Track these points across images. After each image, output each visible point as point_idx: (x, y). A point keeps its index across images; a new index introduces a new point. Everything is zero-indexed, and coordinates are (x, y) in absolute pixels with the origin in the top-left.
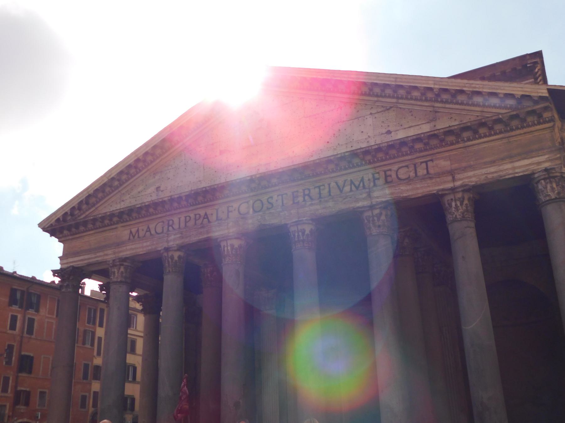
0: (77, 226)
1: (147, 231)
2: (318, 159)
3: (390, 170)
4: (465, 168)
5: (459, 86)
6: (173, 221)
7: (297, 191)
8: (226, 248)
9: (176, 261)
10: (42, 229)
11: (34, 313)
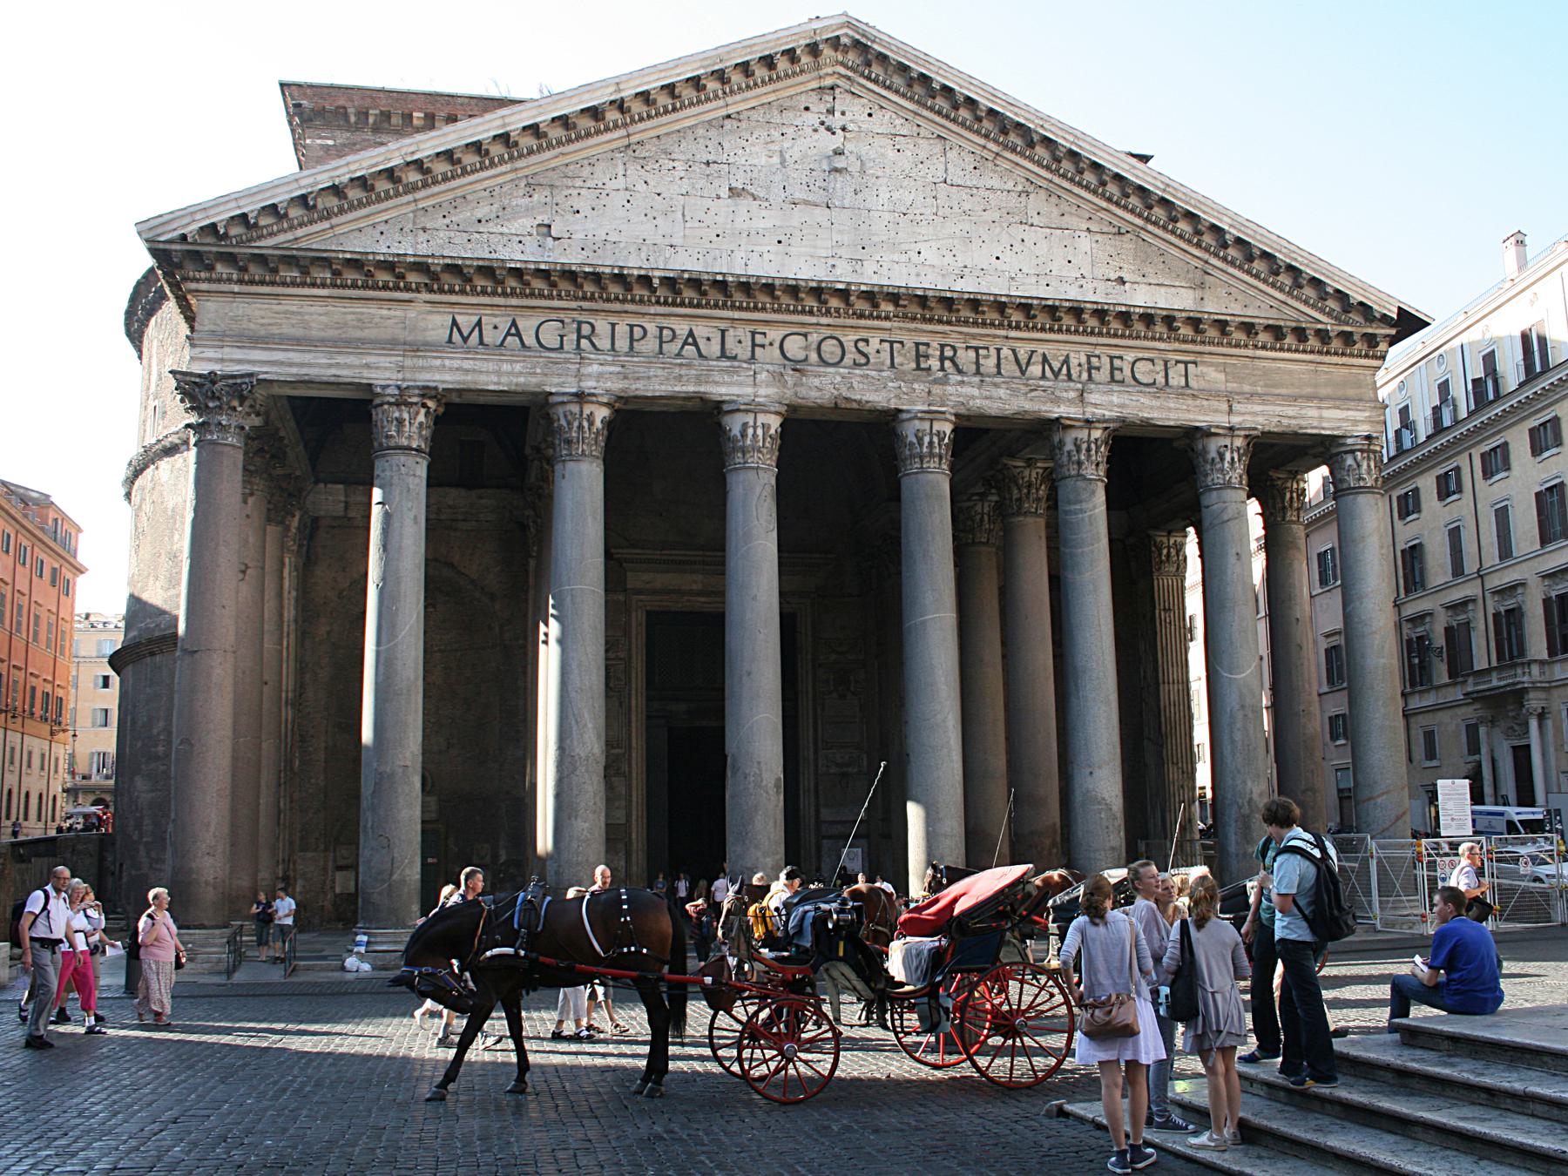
1: (508, 334)
2: (1007, 296)
3: (1121, 358)
5: (1271, 248)
6: (593, 327)
7: (927, 345)
8: (750, 431)
9: (597, 433)
10: (147, 241)
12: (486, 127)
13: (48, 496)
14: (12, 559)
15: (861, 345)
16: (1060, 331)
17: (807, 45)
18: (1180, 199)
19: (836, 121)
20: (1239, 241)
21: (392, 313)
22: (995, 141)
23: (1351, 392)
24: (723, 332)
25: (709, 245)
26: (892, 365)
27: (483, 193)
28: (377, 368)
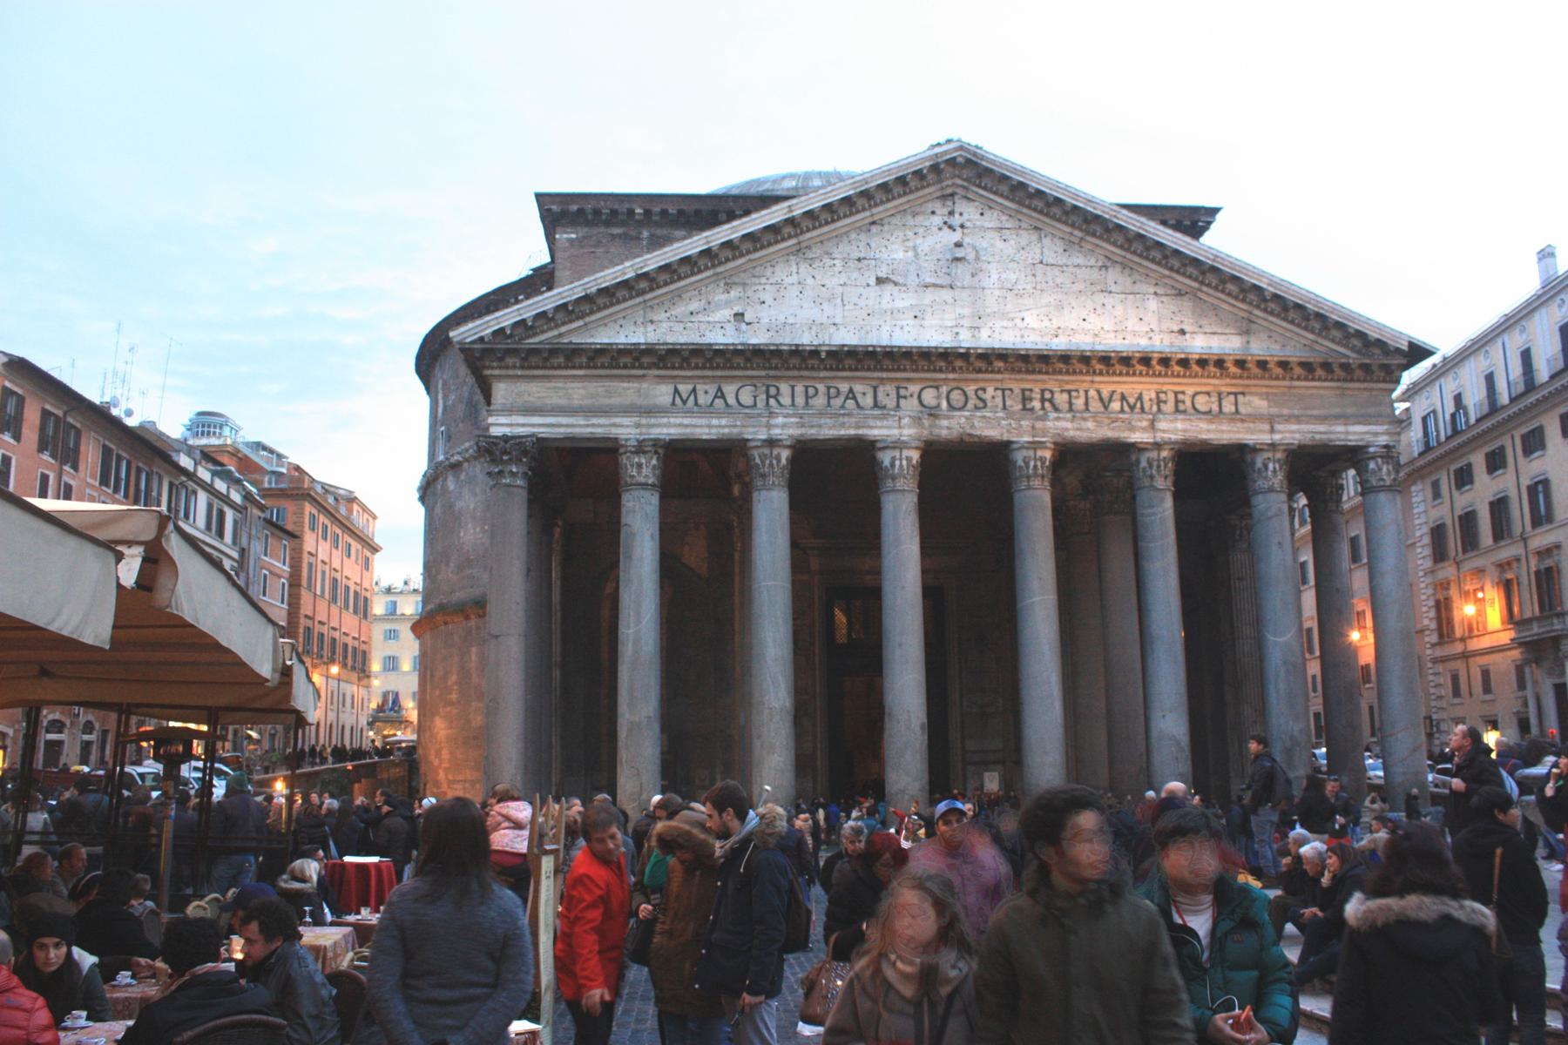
0: (553, 352)
1: (716, 397)
3: (1183, 393)
4: (1290, 416)
5: (1301, 299)
6: (778, 389)
7: (1031, 390)
8: (897, 463)
11: (72, 471)
12: (694, 245)
13: (351, 492)
14: (340, 553)
15: (980, 393)
16: (1134, 374)
17: (931, 166)
18: (1226, 266)
19: (956, 221)
20: (1276, 297)
21: (631, 385)
22: (1080, 229)
23: (1372, 410)
24: (875, 388)
25: (861, 322)
26: (1004, 407)
27: (696, 292)
28: (622, 426)
